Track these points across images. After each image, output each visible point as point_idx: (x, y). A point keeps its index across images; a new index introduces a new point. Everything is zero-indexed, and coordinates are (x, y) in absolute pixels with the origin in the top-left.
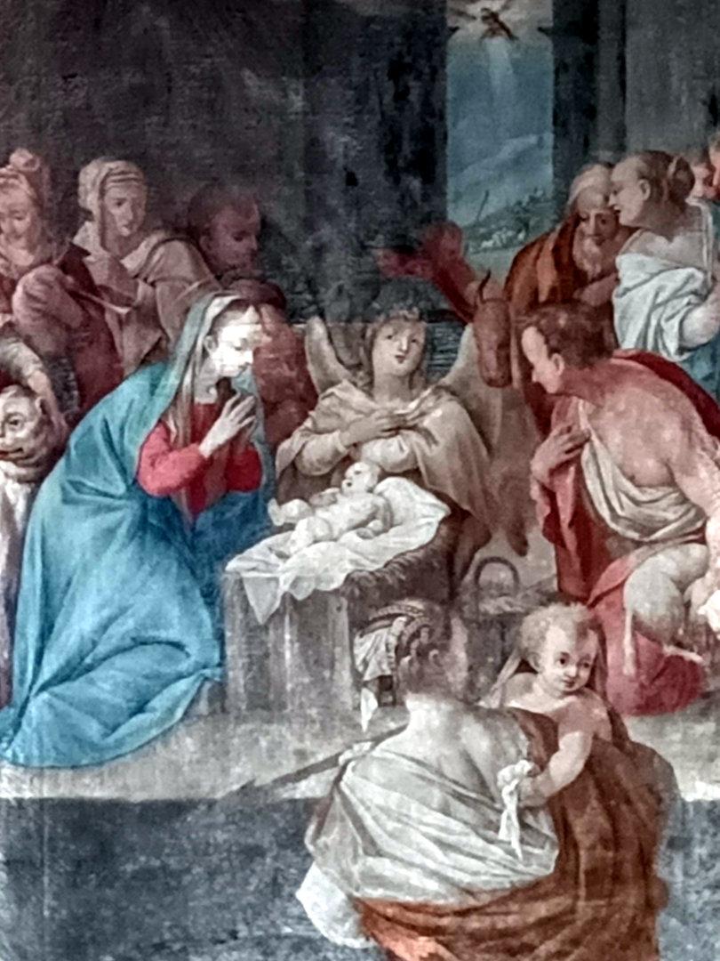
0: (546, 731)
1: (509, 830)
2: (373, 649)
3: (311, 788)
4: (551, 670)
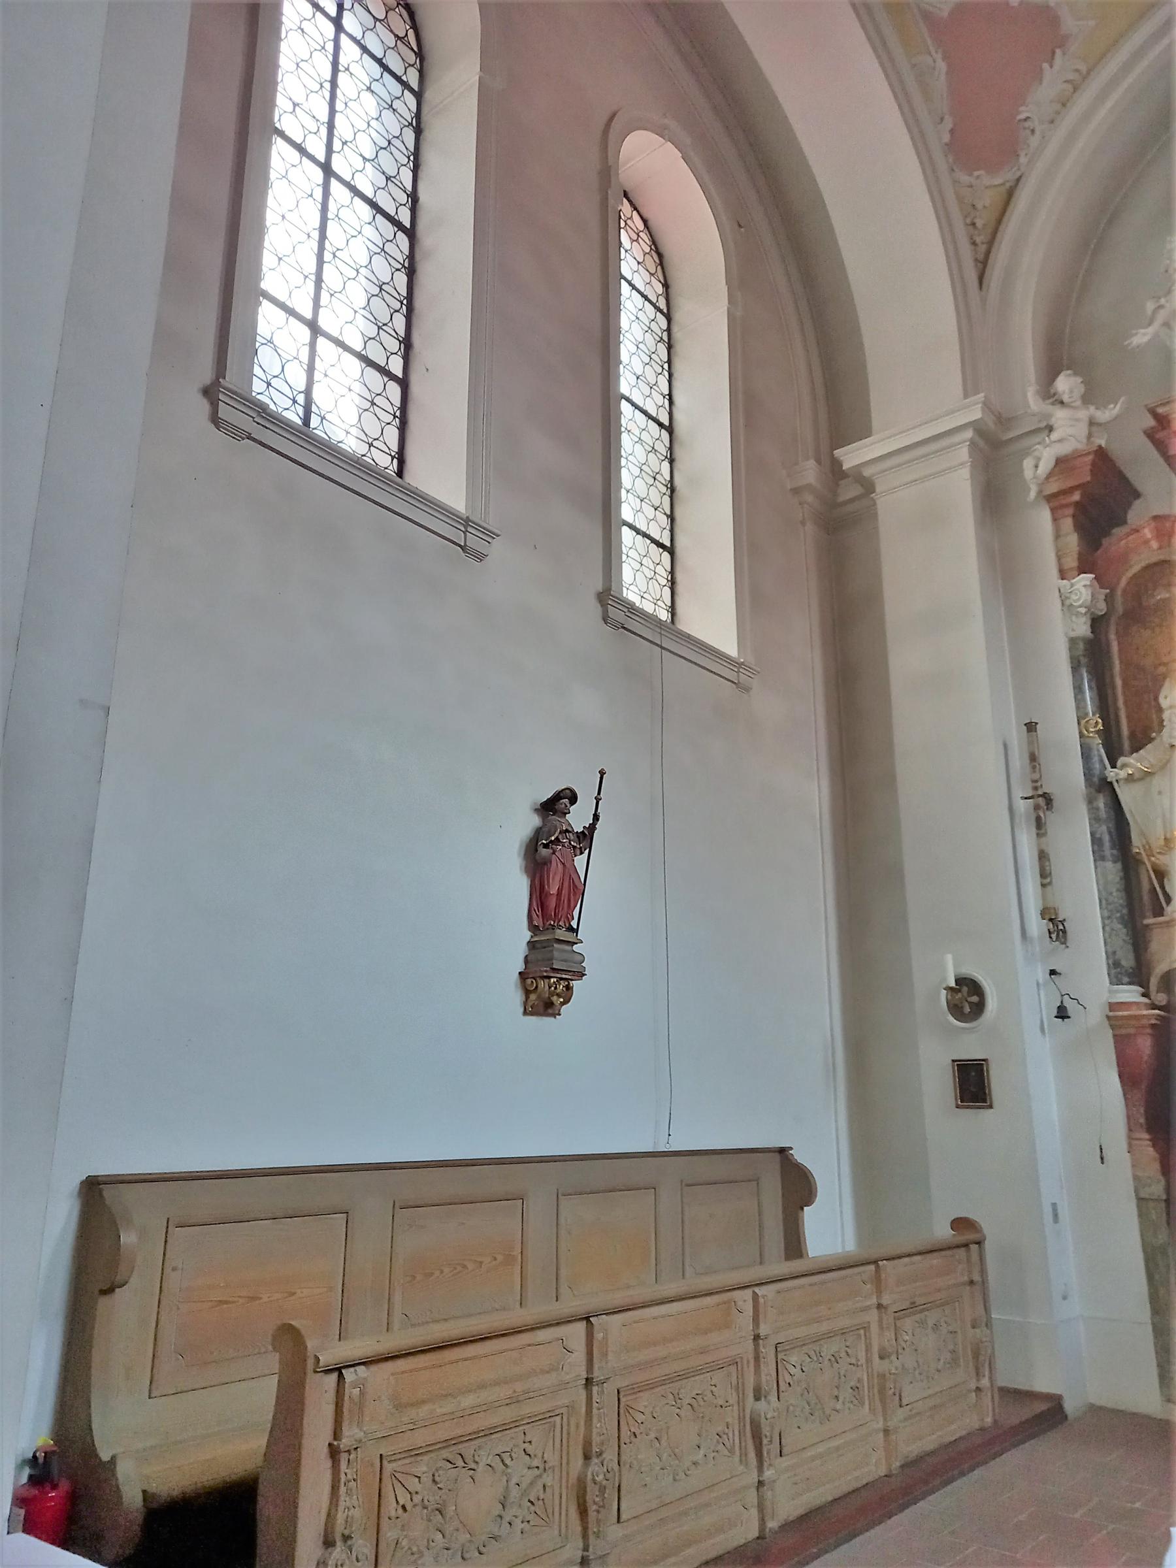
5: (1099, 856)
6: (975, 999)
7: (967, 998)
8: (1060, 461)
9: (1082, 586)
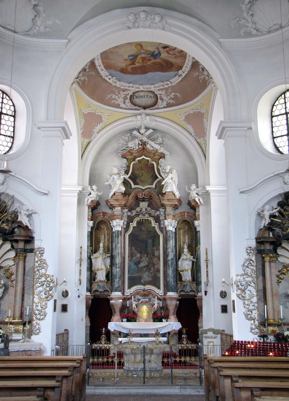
0: (152, 273)
1: (150, 278)
2: (145, 269)
3: (142, 276)
4: (152, 270)
5: (88, 271)
6: (67, 294)
7: (65, 294)
8: (92, 201)
9: (91, 223)
